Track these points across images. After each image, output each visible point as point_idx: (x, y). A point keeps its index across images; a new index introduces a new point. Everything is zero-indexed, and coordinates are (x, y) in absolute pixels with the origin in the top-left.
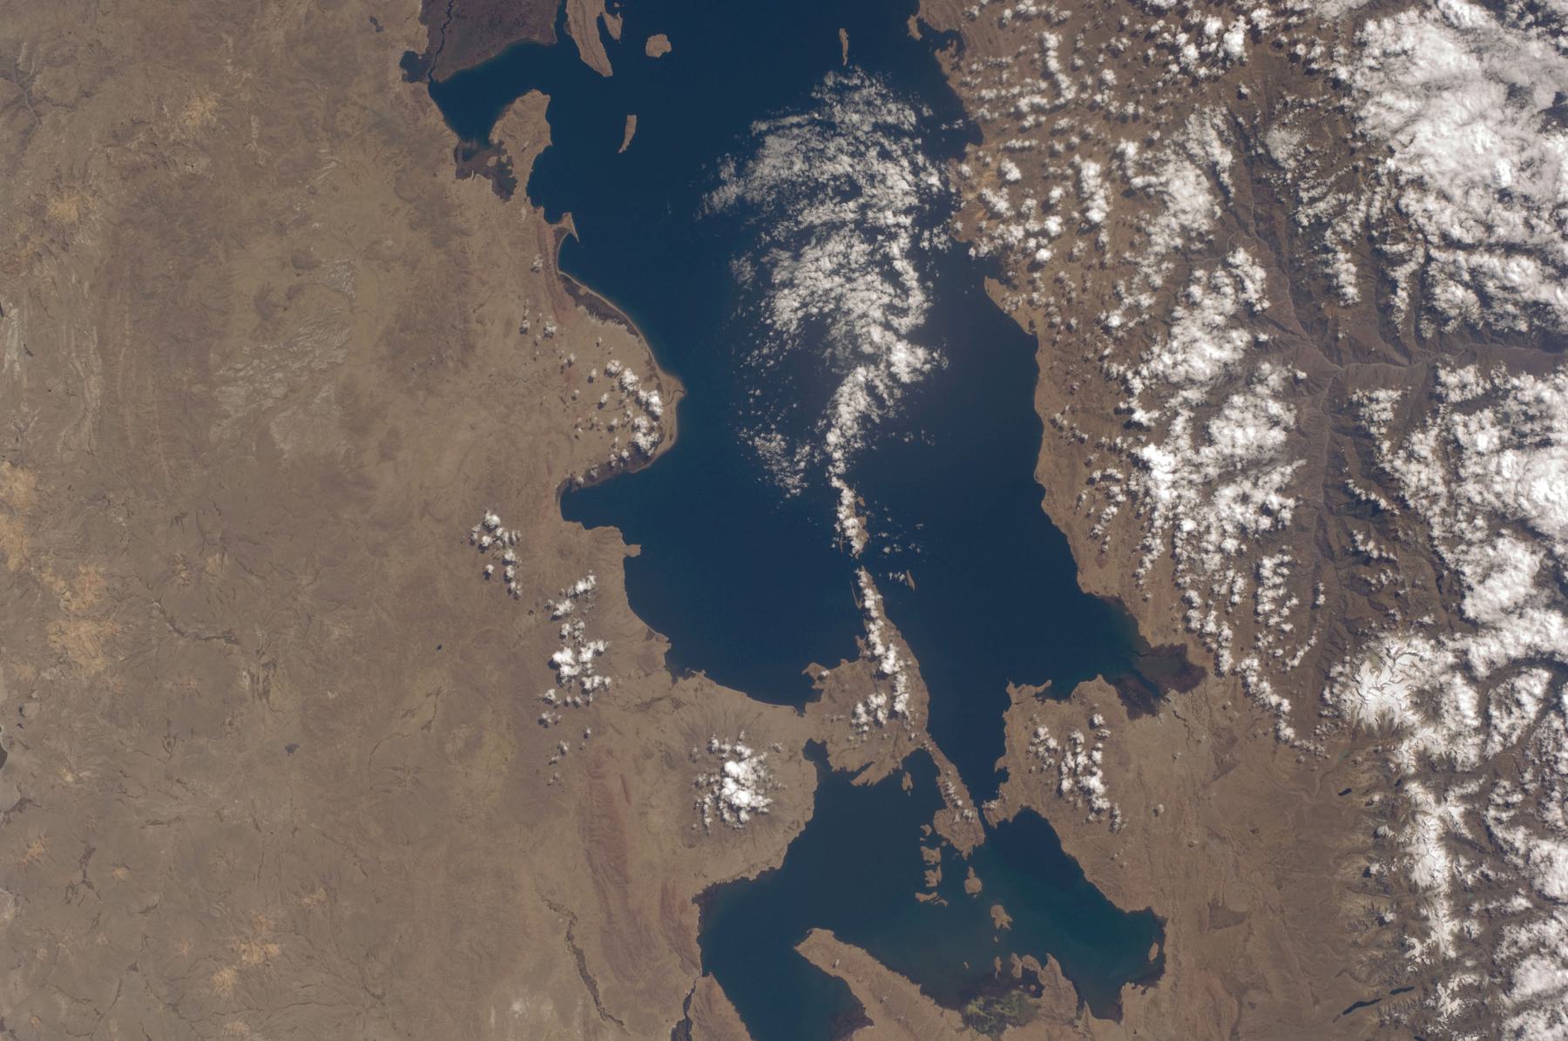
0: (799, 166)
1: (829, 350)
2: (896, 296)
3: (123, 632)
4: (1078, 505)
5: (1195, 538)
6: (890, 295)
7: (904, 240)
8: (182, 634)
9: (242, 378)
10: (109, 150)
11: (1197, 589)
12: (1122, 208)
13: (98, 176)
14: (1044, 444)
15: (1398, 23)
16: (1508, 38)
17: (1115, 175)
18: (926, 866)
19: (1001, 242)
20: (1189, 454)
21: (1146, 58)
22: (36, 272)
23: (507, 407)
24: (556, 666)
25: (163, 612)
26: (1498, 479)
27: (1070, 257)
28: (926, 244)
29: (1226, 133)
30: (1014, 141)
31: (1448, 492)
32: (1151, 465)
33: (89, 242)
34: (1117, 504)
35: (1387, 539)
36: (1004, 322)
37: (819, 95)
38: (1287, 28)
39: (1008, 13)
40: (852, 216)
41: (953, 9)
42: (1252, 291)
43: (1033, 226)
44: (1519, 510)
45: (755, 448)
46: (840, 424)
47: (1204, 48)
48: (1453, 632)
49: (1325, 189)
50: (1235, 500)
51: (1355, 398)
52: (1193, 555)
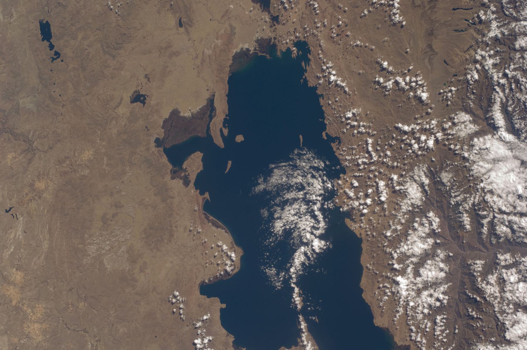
0: (284, 179)
1: (292, 241)
2: (315, 223)
3: (49, 328)
4: (374, 296)
5: (414, 308)
6: (313, 223)
7: (319, 205)
8: (69, 329)
9: (95, 243)
10: (57, 166)
11: (414, 326)
12: (392, 197)
14: (364, 275)
15: (485, 139)
16: (521, 145)
17: (390, 185)
19: (351, 206)
20: (413, 280)
21: (401, 148)
24: (195, 344)
25: (63, 321)
26: (517, 292)
27: (374, 212)
28: (326, 206)
29: (427, 173)
30: (356, 173)
31: (501, 296)
32: (399, 283)
33: (48, 196)
34: (388, 296)
35: (480, 311)
36: (352, 233)
37: (292, 156)
38: (448, 140)
39: (356, 131)
40: (301, 196)
41: (337, 129)
42: (435, 226)
43: (362, 201)
44: (525, 303)
45: (266, 273)
46: (295, 266)
47: (420, 145)
48: (502, 344)
49: (460, 193)
50: (428, 296)
51: (469, 263)
52: (413, 314)
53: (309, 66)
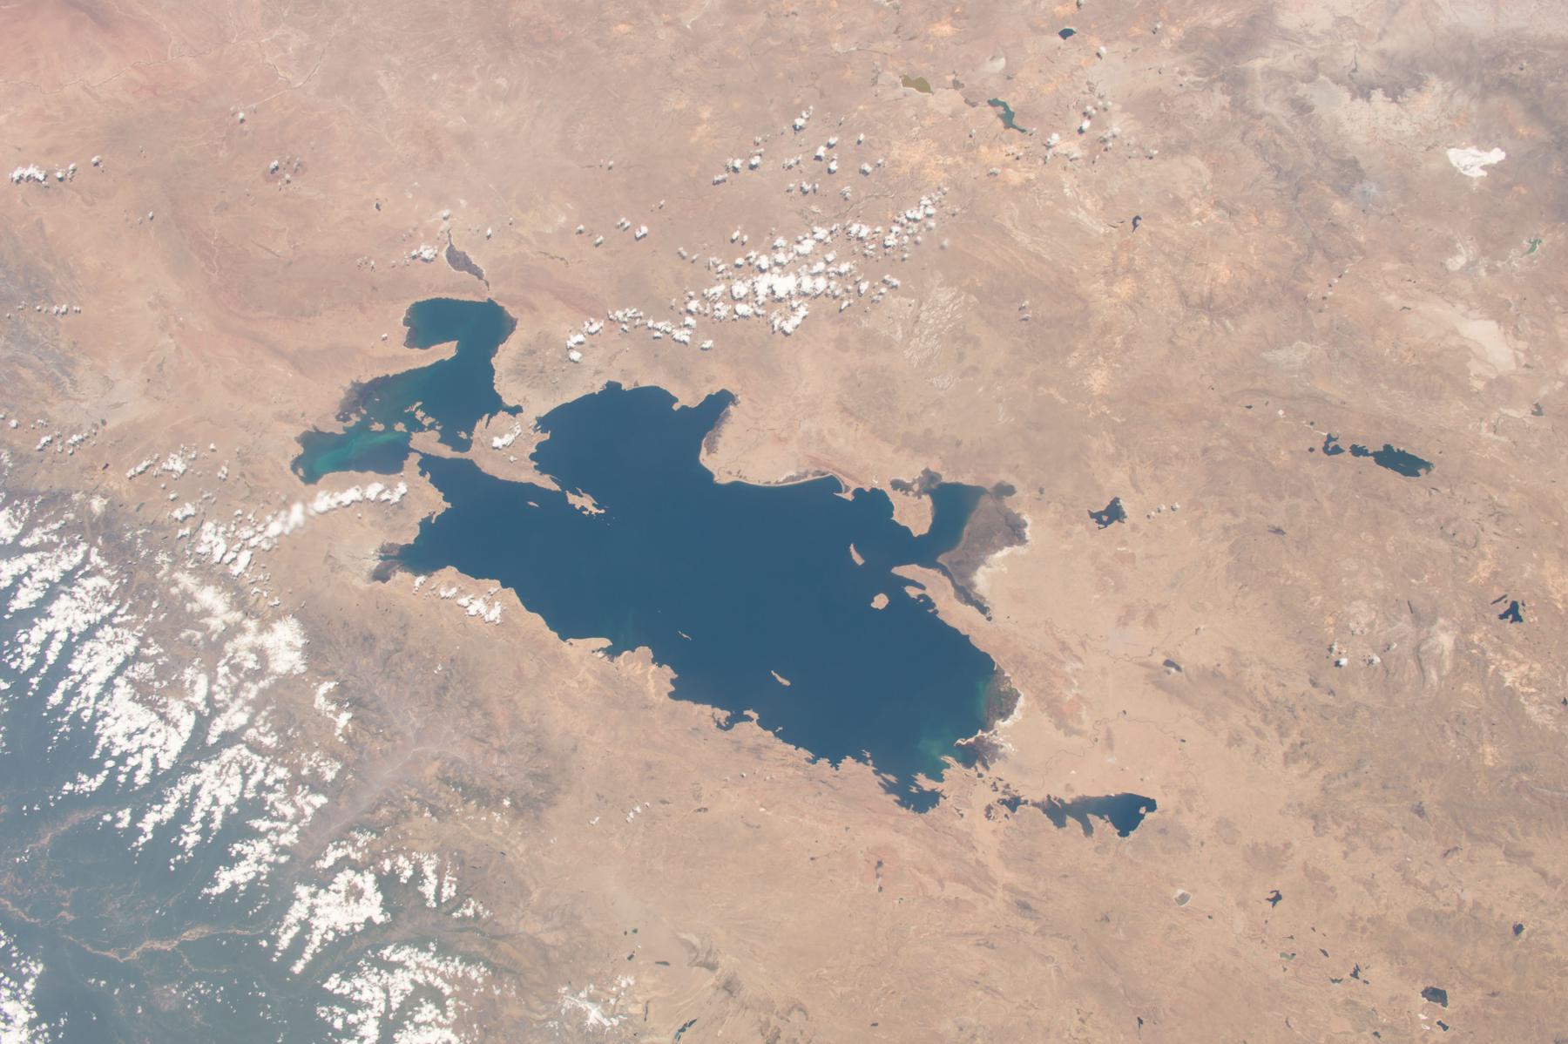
10: (1130, 327)
13: (1123, 313)
18: (427, 415)
22: (1109, 253)
25: (886, 196)
53: (880, 784)
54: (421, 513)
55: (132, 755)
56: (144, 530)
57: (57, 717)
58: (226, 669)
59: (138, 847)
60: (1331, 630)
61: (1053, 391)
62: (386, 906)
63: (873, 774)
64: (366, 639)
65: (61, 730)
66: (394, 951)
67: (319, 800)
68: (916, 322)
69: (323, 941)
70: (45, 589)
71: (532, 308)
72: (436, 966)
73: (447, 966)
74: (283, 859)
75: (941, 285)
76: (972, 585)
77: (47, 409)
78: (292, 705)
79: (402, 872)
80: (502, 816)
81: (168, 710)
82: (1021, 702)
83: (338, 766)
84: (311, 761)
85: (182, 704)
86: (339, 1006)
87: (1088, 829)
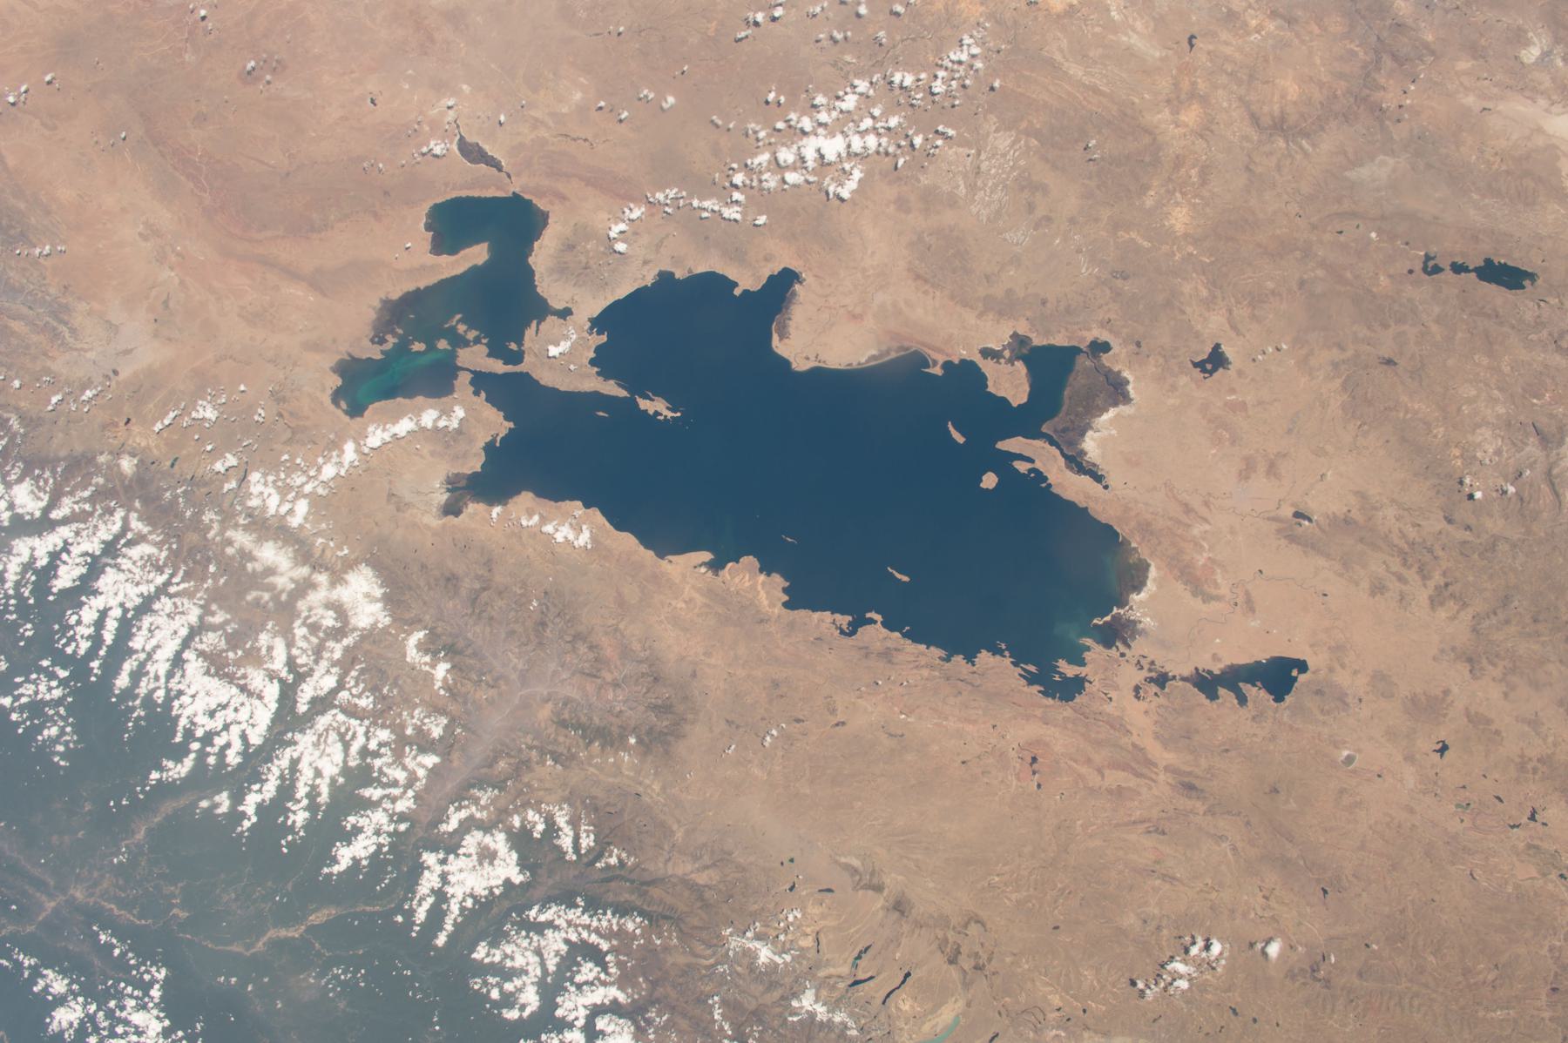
9: (1009, 151)
10: (1204, 157)
13: (1193, 143)
18: (471, 328)
22: (1169, 78)
23: (869, 276)
25: (923, 38)
53: (1020, 675)
54: (483, 439)
55: (218, 734)
56: (184, 488)
57: (127, 702)
58: (304, 631)
59: (243, 832)
60: (1459, 462)
61: (1133, 235)
62: (523, 864)
63: (1012, 667)
64: (448, 580)
65: (135, 715)
66: (540, 911)
67: (431, 760)
68: (978, 173)
69: (463, 909)
70: (86, 563)
71: (563, 198)
72: (588, 922)
73: (600, 920)
74: (403, 827)
75: (997, 131)
76: (1083, 453)
77: (49, 363)
78: (382, 662)
79: (534, 827)
80: (630, 755)
81: (248, 681)
82: (1153, 572)
83: (444, 721)
84: (413, 719)
85: (262, 672)
86: (494, 976)
87: (1242, 700)
